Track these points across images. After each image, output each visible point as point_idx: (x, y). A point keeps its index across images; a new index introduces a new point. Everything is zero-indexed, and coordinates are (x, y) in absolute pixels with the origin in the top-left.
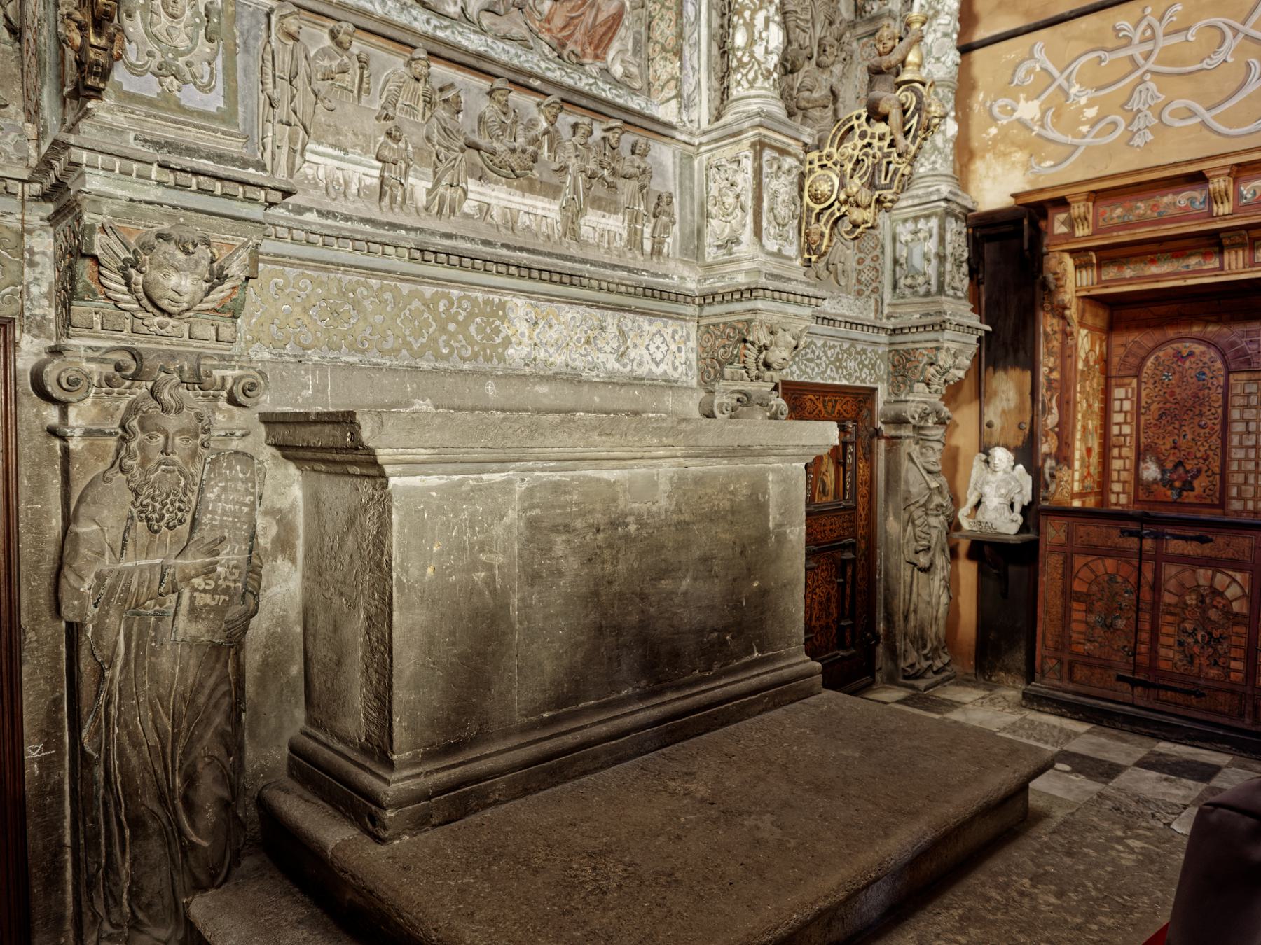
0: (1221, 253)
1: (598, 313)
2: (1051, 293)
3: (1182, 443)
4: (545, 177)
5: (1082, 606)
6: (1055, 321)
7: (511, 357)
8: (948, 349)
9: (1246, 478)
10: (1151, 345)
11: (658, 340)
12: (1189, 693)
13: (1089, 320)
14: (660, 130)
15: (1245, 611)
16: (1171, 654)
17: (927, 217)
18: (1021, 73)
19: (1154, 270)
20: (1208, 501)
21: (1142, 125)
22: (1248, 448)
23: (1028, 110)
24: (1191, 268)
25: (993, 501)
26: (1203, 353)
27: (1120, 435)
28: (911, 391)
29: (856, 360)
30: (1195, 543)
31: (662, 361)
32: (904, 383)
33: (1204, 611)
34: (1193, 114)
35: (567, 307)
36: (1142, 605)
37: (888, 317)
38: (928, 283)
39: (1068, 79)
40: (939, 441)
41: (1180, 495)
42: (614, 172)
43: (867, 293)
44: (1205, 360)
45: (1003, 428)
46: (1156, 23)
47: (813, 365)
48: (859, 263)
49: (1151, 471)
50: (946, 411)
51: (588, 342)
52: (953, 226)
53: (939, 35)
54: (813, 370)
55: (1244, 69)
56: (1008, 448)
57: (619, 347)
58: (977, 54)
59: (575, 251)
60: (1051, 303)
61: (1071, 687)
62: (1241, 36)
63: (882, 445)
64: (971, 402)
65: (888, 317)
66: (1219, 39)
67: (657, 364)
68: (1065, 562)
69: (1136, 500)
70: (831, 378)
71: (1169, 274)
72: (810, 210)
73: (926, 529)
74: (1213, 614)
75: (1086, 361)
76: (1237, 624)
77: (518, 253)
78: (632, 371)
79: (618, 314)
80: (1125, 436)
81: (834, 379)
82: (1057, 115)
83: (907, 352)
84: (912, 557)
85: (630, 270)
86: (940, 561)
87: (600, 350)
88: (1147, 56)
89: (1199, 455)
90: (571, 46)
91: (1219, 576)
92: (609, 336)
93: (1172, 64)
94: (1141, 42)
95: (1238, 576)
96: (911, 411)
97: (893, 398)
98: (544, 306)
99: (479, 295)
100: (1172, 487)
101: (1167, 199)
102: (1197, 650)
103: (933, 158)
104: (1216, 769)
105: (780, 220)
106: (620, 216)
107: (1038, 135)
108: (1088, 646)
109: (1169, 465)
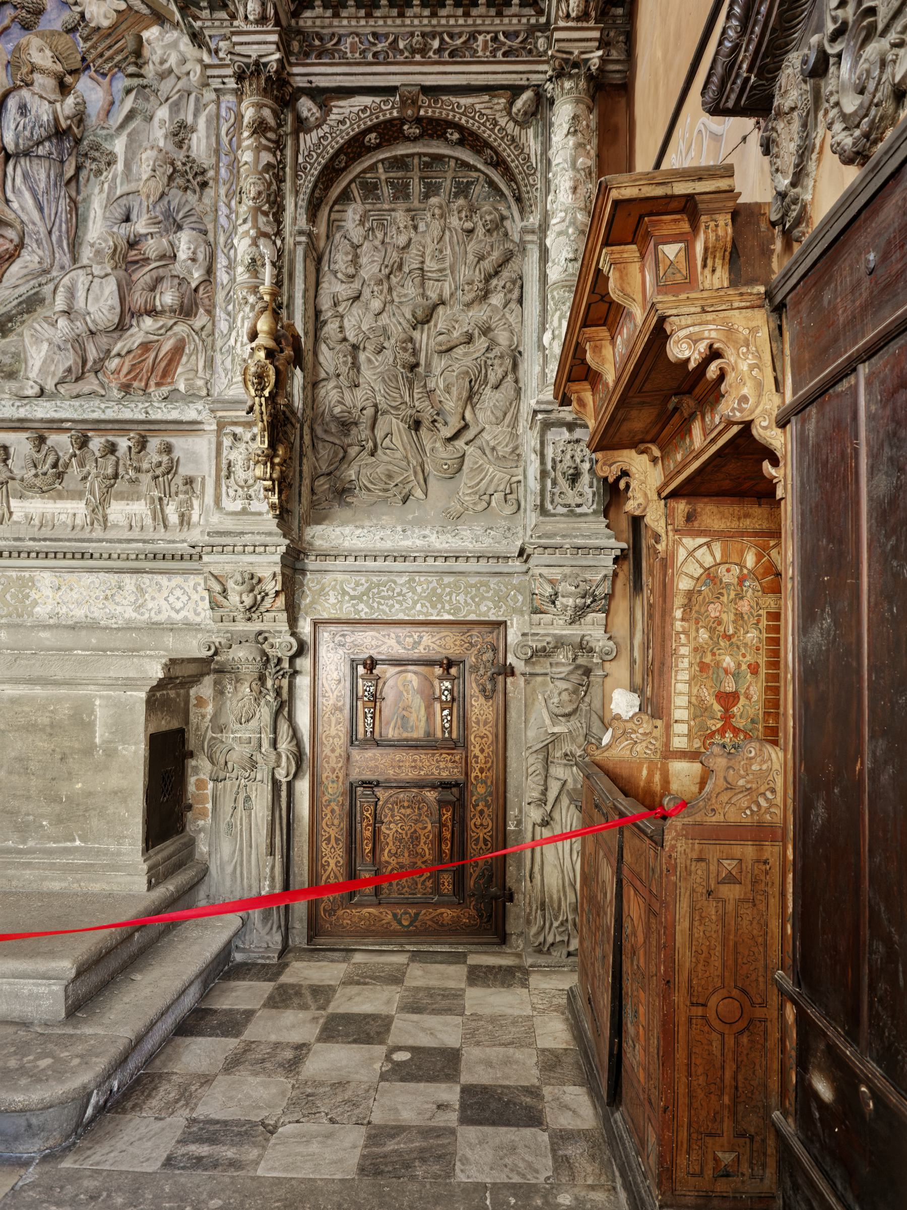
1: (116, 575)
4: (72, 486)
7: (38, 613)
11: (178, 592)
14: (191, 427)
31: (182, 609)
35: (87, 575)
42: (138, 470)
47: (391, 602)
51: (106, 598)
57: (137, 600)
59: (98, 533)
67: (178, 612)
77: (43, 543)
78: (150, 618)
79: (135, 576)
85: (144, 541)
87: (117, 604)
90: (136, 384)
92: (125, 593)
98: (67, 576)
99: (14, 574)
105: (242, 483)
106: (143, 501)
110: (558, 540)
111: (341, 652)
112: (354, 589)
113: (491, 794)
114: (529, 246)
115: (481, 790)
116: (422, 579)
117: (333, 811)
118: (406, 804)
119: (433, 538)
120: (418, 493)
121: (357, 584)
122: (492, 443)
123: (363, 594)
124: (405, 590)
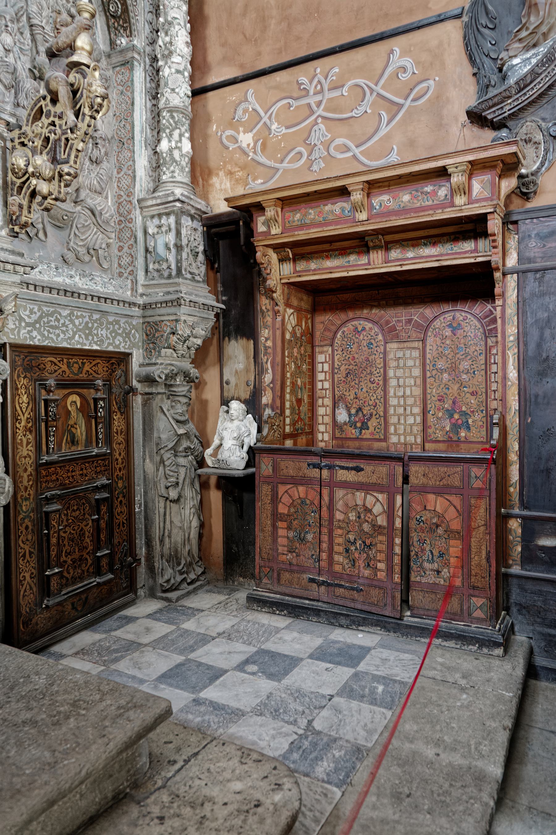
0: (368, 252)
2: (265, 280)
3: (361, 395)
5: (285, 525)
6: (267, 301)
8: (185, 321)
9: (399, 420)
10: (339, 322)
12: (353, 589)
13: (295, 302)
15: (385, 524)
16: (341, 559)
17: (168, 214)
18: (240, 112)
19: (329, 263)
20: (377, 437)
21: (317, 156)
22: (399, 397)
23: (246, 139)
24: (351, 264)
25: (228, 443)
26: (371, 329)
27: (322, 389)
28: (159, 355)
29: (108, 329)
30: (353, 472)
32: (154, 349)
33: (361, 525)
34: (348, 150)
36: (323, 522)
37: (142, 295)
38: (169, 268)
39: (270, 118)
40: (185, 396)
41: (361, 433)
43: (126, 275)
44: (372, 334)
45: (236, 385)
46: (323, 81)
47: (57, 331)
48: (119, 251)
49: (342, 416)
50: (194, 372)
52: (186, 222)
53: (173, 70)
54: (58, 335)
55: (377, 118)
56: (240, 401)
58: (210, 94)
60: (264, 288)
61: (279, 589)
62: (375, 94)
63: (138, 400)
64: (214, 365)
65: (142, 295)
66: (362, 95)
68: (272, 490)
69: (334, 437)
70: (78, 342)
71: (337, 267)
72: (13, 183)
73: (173, 468)
74: (366, 527)
75: (293, 333)
76: (380, 534)
80: (326, 389)
81: (83, 344)
82: (264, 145)
83: (156, 323)
84: (163, 491)
86: (188, 493)
88: (319, 104)
89: (371, 403)
91: (368, 496)
93: (334, 111)
94: (314, 94)
95: (380, 496)
96: (158, 372)
97: (147, 361)
100: (356, 428)
101: (329, 207)
102: (357, 555)
103: (172, 168)
104: (365, 651)
107: (252, 159)
108: (289, 556)
109: (353, 411)
110: (193, 298)
111: (28, 375)
112: (29, 317)
113: (125, 488)
114: (136, 63)
115: (120, 484)
116: (79, 314)
117: (27, 528)
118: (75, 508)
119: (77, 279)
120: (41, 235)
121: (32, 312)
122: (99, 208)
123: (36, 322)
124: (67, 322)
